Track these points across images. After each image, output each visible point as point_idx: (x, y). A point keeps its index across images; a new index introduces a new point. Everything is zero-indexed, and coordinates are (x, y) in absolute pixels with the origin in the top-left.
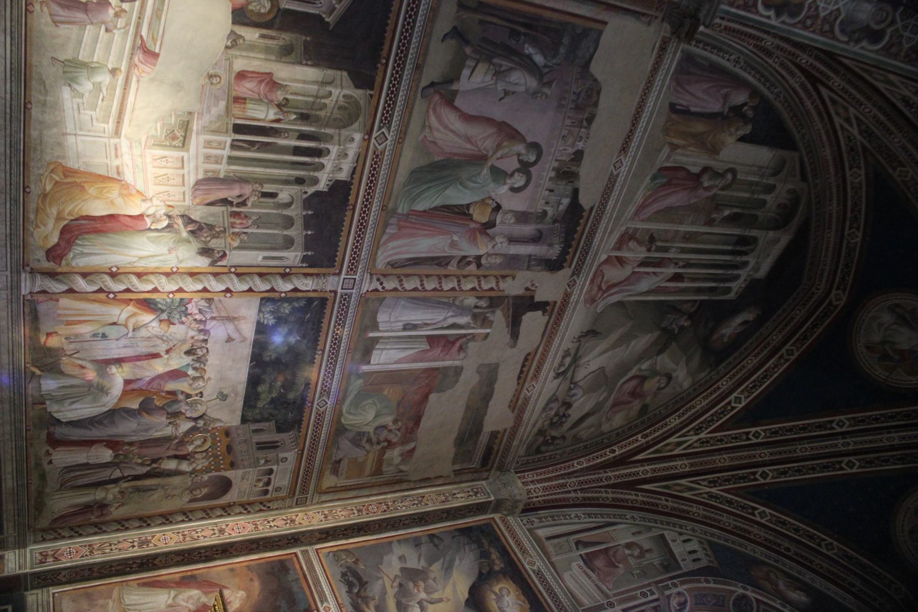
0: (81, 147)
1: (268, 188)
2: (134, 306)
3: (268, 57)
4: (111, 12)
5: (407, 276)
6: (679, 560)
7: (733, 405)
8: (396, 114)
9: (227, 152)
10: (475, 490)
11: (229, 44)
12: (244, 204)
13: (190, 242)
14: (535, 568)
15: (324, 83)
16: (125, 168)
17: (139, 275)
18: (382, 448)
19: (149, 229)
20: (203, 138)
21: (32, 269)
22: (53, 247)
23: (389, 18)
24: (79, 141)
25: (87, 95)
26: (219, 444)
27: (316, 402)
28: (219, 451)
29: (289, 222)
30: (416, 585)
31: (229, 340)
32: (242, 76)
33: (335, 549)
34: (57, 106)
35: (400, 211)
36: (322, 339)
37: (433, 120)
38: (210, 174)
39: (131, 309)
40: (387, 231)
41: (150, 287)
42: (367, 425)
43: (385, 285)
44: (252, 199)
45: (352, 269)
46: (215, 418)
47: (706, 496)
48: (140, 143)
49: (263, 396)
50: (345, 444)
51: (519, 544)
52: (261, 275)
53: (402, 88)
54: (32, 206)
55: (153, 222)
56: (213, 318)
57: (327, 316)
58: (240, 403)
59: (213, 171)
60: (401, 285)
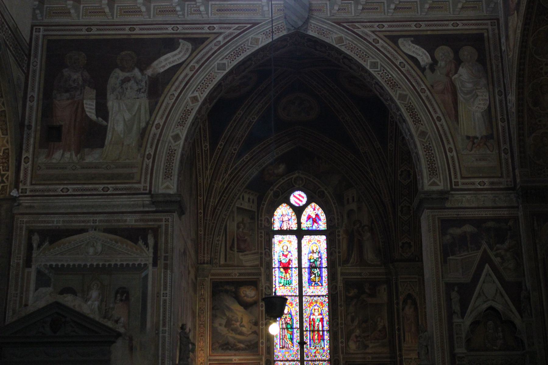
6: (251, 209)
7: (206, 149)
10: (201, 284)
14: (238, 274)
30: (233, 324)
33: (211, 349)
47: (229, 177)
51: (226, 275)
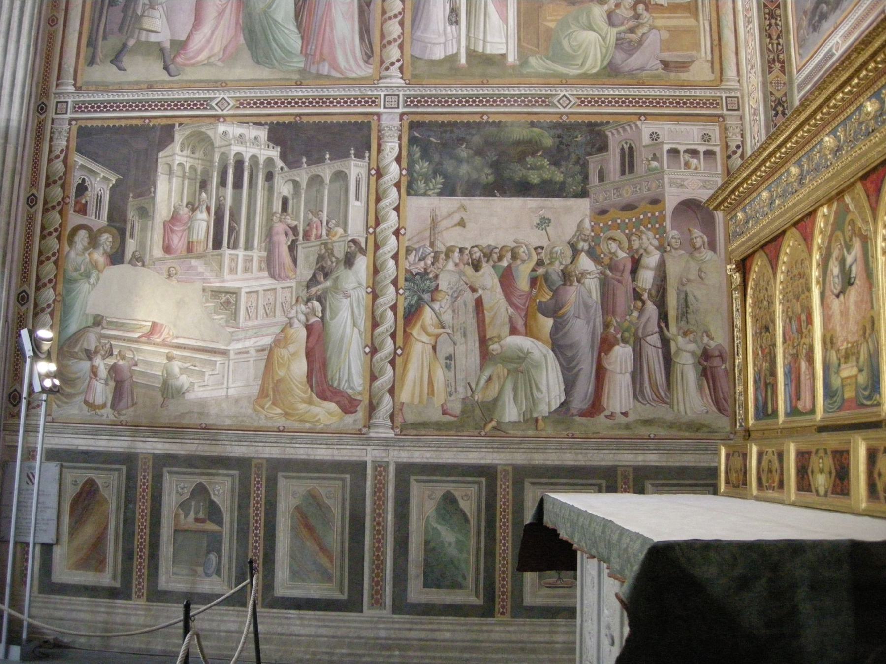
0: (239, 384)
1: (277, 206)
2: (412, 328)
3: (150, 228)
4: (121, 362)
5: (383, 36)
8: (197, 96)
9: (241, 253)
11: (140, 264)
12: (295, 229)
13: (337, 278)
15: (170, 172)
16: (260, 343)
17: (375, 325)
18: (647, 10)
19: (323, 318)
20: (227, 276)
21: (365, 427)
22: (340, 407)
23: (109, 126)
24: (234, 385)
25: (191, 380)
26: (619, 221)
27: (562, 110)
28: (630, 220)
29: (316, 180)
31: (462, 224)
32: (167, 249)
34: (203, 404)
35: (302, 65)
36: (465, 119)
37: (202, 56)
38: (264, 265)
39: (416, 331)
40: (326, 73)
41: (390, 314)
42: (604, 39)
43: (394, 60)
44: (289, 221)
45: (373, 102)
46: (574, 228)
48: (234, 332)
49: (546, 176)
50: (635, 61)
52: (378, 200)
53: (172, 97)
54: (297, 425)
55: (315, 315)
56: (432, 245)
57: (433, 118)
58: (556, 202)
59: (260, 262)
60: (395, 40)
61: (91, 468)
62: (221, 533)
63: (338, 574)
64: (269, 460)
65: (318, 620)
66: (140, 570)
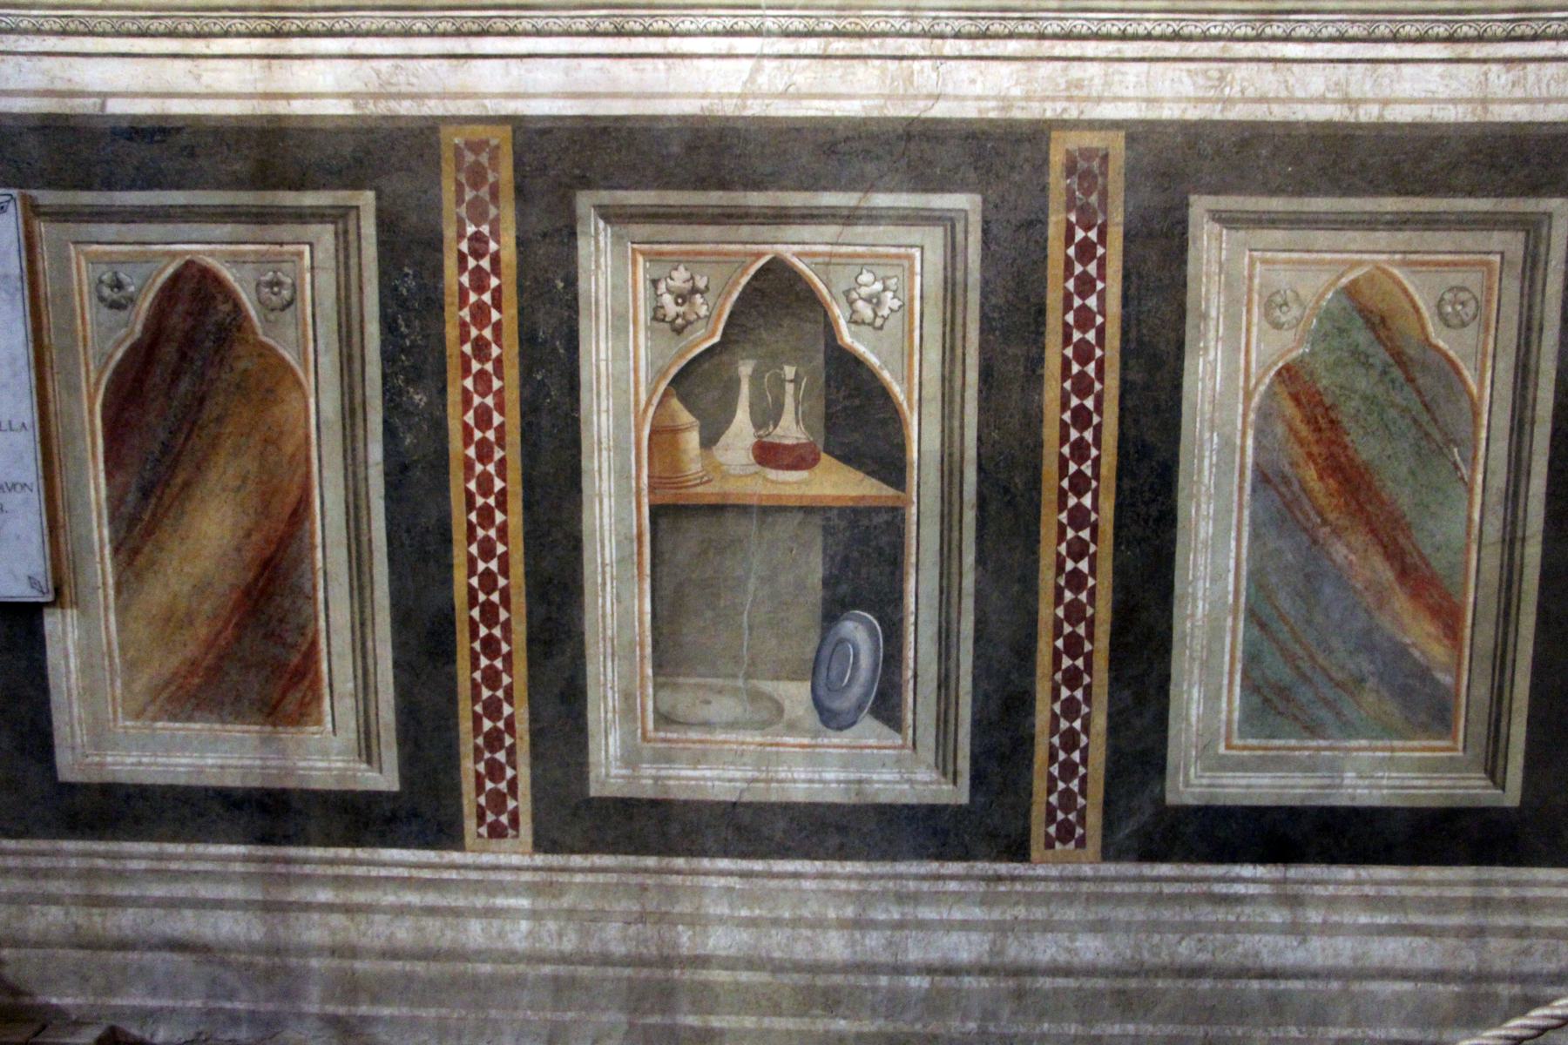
61: (189, 214)
62: (896, 514)
63: (1482, 691)
64: (1138, 133)
65: (1368, 903)
66: (493, 709)
